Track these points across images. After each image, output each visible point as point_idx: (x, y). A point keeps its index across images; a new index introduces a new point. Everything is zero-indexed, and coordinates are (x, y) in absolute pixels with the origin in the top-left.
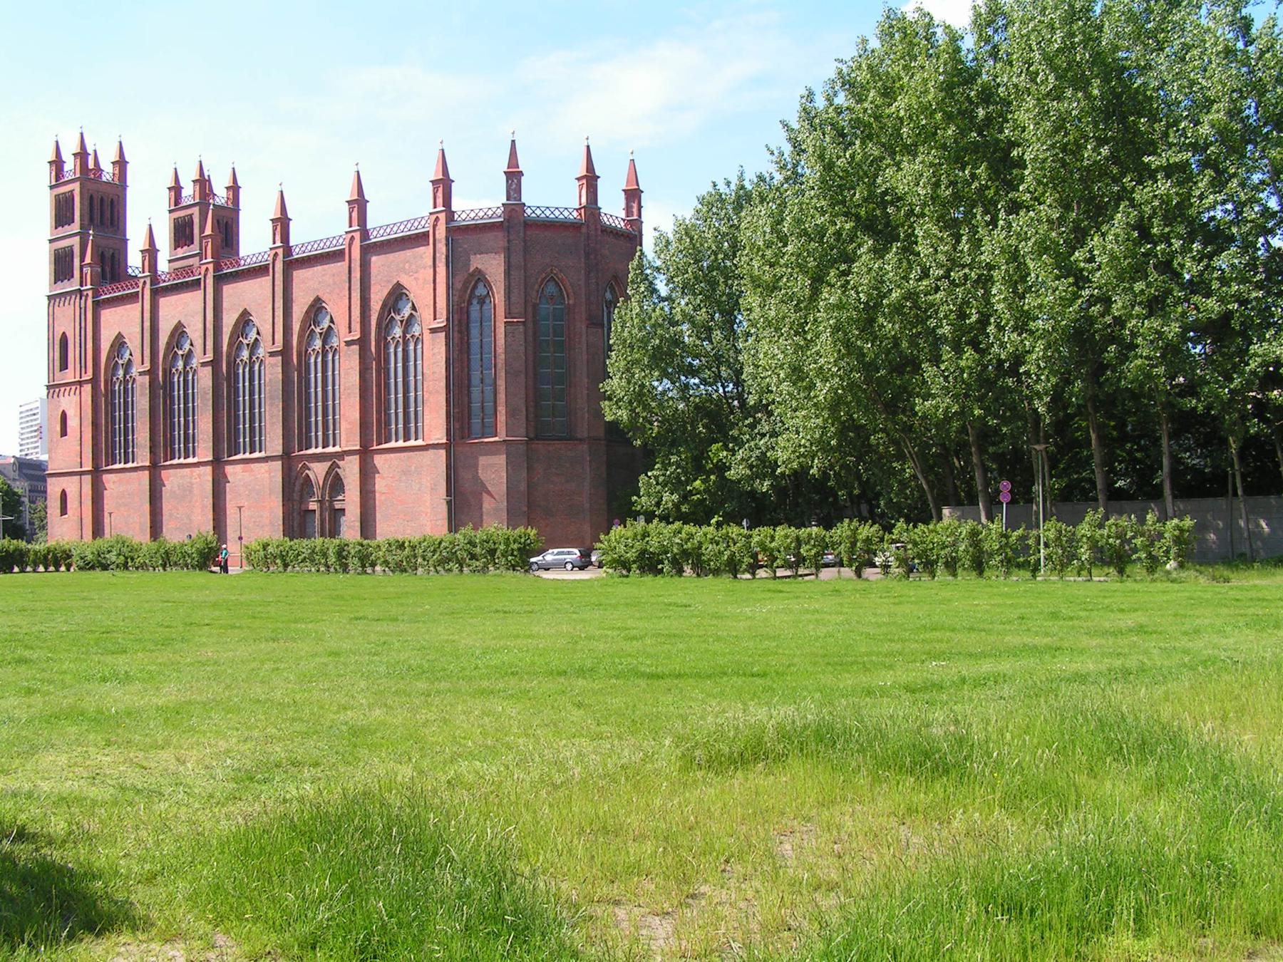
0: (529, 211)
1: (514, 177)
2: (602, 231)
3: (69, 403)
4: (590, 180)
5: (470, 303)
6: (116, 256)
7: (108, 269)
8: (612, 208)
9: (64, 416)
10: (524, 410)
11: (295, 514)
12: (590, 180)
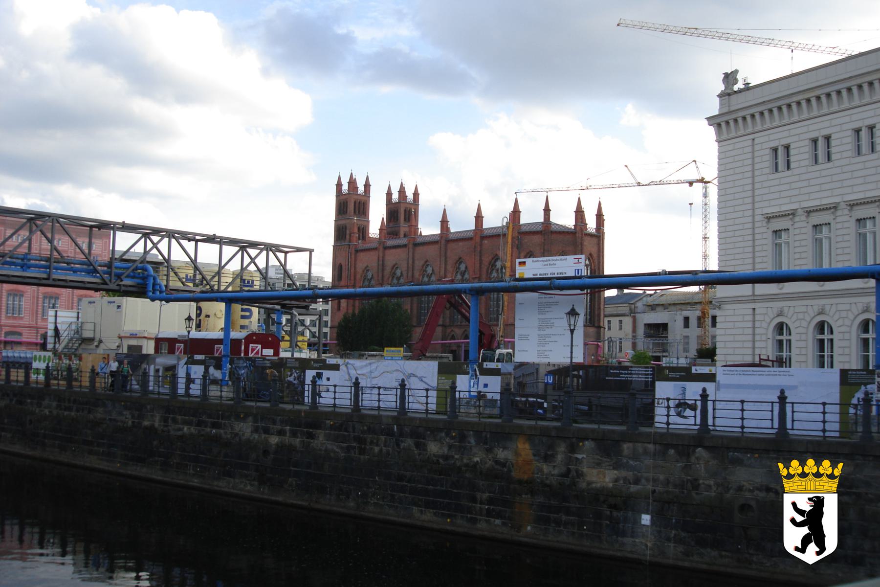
0: (553, 227)
1: (547, 210)
4: (579, 213)
7: (361, 235)
8: (591, 224)
12: (579, 213)
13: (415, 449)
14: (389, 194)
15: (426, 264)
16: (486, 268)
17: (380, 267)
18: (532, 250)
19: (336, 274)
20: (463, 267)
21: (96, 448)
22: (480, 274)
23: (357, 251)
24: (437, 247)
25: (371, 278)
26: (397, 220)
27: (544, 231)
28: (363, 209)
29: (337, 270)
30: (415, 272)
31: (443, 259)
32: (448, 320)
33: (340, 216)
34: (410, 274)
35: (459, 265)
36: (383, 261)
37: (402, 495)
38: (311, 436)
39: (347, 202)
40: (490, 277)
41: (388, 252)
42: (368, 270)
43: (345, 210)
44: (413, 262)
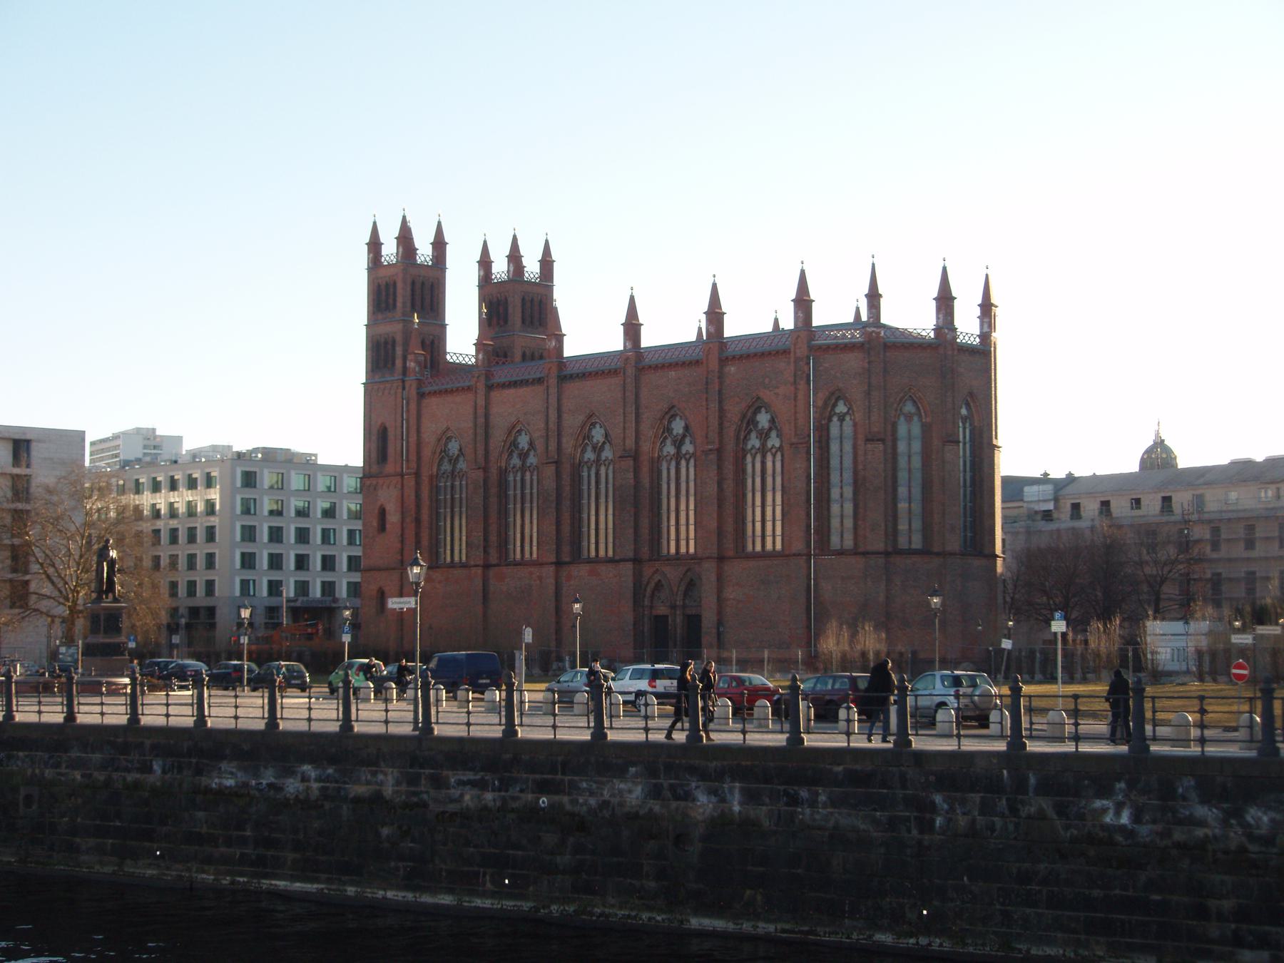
1: (874, 297)
2: (958, 350)
3: (389, 497)
4: (945, 301)
5: (830, 420)
6: (436, 342)
7: (429, 357)
8: (967, 325)
9: (382, 513)
10: (883, 525)
11: (646, 619)
12: (945, 301)
13: (1055, 817)
14: (485, 263)
15: (590, 421)
16: (735, 426)
17: (481, 431)
18: (841, 385)
19: (374, 446)
20: (678, 427)
21: (223, 849)
22: (721, 441)
24: (615, 381)
26: (506, 322)
27: (869, 342)
28: (432, 301)
29: (374, 438)
30: (564, 440)
31: (631, 409)
32: (645, 550)
33: (380, 316)
34: (553, 446)
35: (670, 422)
36: (487, 416)
37: (1028, 910)
38: (794, 801)
41: (496, 395)
42: (449, 439)
43: (391, 301)
44: (559, 417)
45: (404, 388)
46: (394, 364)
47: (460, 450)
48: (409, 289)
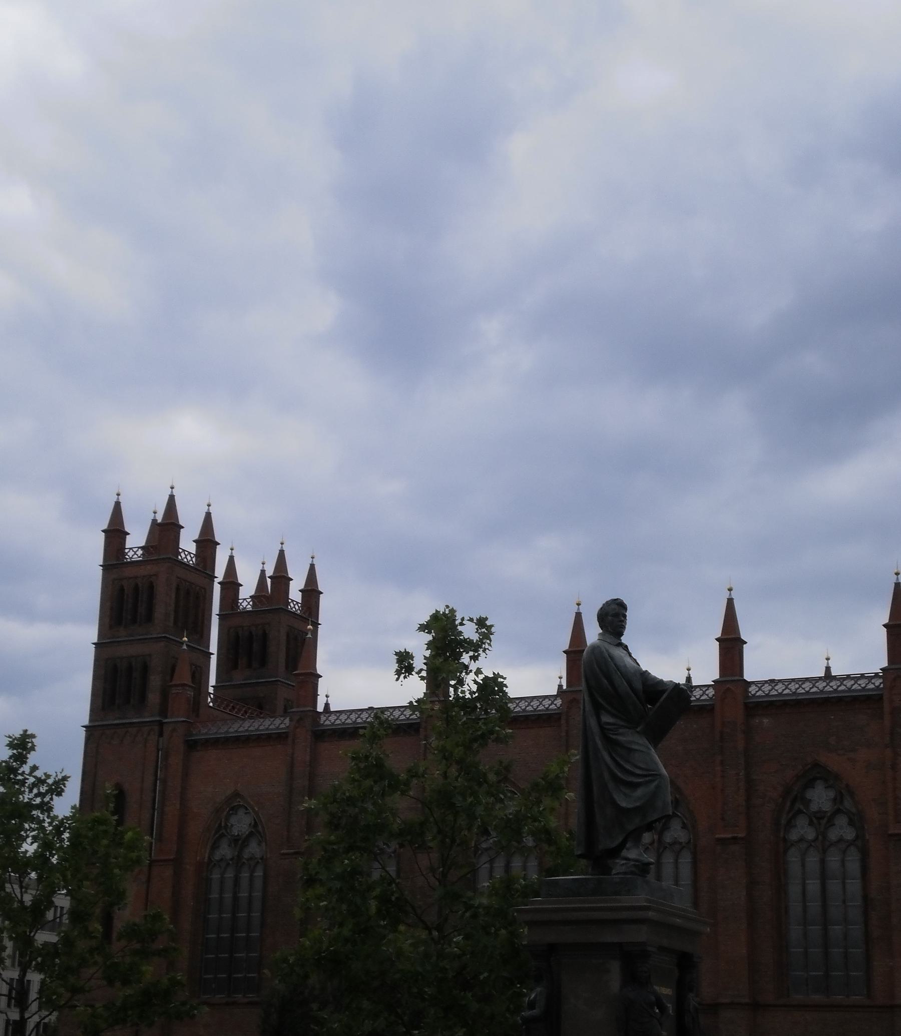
23: (192, 745)
25: (251, 834)
39: (151, 587)
40: (785, 840)
45: (161, 734)
46: (143, 698)
47: (256, 825)
48: (173, 596)
